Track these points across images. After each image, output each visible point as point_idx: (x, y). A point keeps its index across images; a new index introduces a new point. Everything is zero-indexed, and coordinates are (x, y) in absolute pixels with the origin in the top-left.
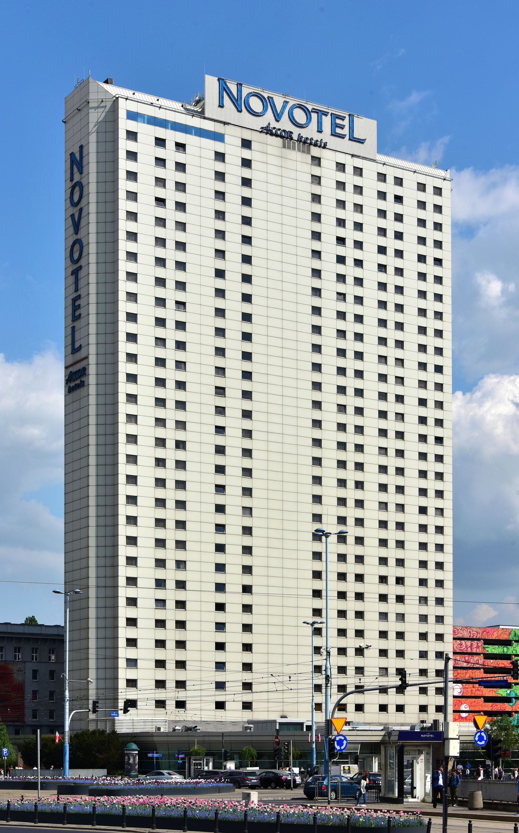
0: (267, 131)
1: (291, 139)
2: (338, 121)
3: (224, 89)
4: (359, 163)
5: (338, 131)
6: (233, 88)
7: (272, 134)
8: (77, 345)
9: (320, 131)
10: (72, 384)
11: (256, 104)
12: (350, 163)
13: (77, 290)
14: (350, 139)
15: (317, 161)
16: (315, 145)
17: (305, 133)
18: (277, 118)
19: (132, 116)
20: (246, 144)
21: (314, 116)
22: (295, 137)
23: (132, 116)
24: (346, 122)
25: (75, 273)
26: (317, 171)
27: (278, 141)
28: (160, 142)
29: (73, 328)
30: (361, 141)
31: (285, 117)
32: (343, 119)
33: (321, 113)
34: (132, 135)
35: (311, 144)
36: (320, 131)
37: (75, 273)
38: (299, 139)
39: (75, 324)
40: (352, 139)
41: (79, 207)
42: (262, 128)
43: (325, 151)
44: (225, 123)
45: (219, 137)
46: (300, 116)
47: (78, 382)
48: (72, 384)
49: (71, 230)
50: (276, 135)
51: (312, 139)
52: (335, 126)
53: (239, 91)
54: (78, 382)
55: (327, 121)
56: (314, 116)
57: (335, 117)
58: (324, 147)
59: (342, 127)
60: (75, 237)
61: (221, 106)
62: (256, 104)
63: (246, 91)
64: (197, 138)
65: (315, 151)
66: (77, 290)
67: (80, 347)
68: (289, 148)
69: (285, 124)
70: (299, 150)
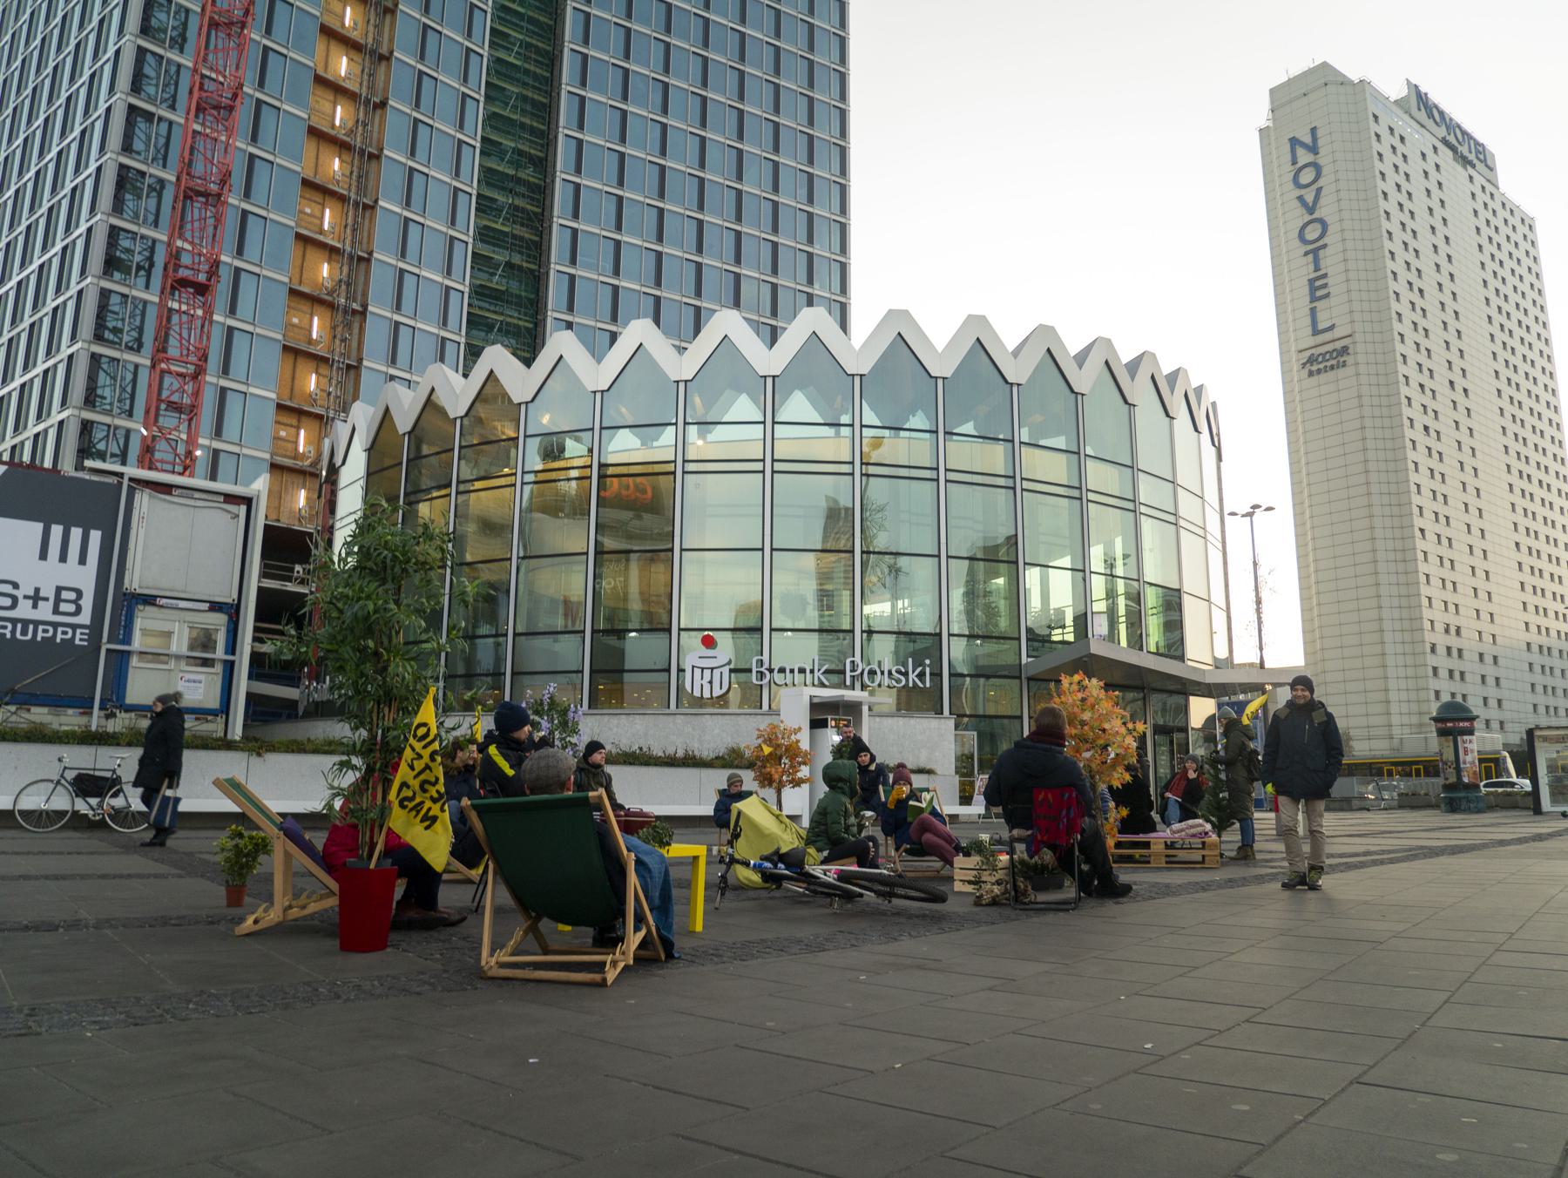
8: (1321, 326)
10: (1314, 368)
13: (1317, 269)
27: (1450, 153)
29: (1313, 311)
39: (1319, 305)
47: (1334, 362)
48: (1314, 368)
49: (1301, 211)
52: (1478, 152)
54: (1334, 362)
60: (1308, 218)
67: (1332, 328)
69: (1451, 139)
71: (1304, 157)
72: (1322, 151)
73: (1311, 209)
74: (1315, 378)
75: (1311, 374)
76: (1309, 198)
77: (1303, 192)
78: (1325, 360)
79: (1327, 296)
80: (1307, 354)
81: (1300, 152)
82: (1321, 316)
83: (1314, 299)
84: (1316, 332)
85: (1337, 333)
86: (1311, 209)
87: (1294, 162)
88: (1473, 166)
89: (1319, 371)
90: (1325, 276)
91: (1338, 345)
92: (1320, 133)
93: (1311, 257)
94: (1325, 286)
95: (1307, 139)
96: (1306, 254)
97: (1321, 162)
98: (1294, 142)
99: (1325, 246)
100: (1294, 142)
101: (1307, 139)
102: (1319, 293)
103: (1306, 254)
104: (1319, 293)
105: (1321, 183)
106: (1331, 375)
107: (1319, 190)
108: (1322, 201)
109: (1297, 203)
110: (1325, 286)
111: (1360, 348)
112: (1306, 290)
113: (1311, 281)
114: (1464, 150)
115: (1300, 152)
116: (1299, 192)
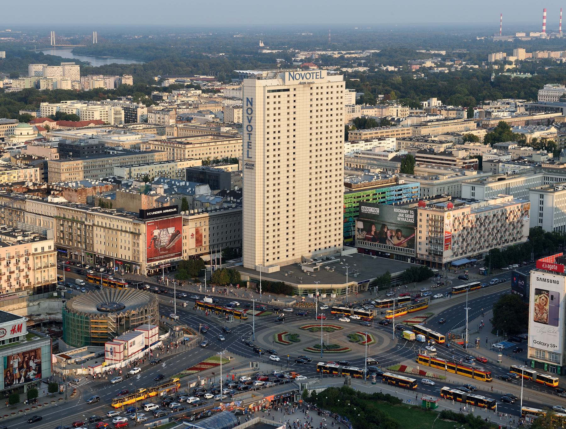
0: (300, 83)
3: (290, 74)
5: (318, 77)
6: (292, 73)
8: (250, 156)
15: (311, 88)
17: (309, 81)
18: (303, 79)
19: (269, 91)
20: (295, 89)
23: (269, 91)
24: (319, 74)
25: (250, 134)
27: (302, 86)
37: (250, 134)
45: (288, 90)
49: (247, 121)
52: (316, 75)
55: (315, 75)
62: (297, 77)
65: (311, 86)
69: (305, 80)
71: (249, 106)
73: (250, 122)
76: (250, 118)
82: (250, 153)
83: (248, 148)
84: (248, 157)
85: (252, 160)
86: (250, 122)
88: (313, 83)
91: (253, 163)
92: (253, 100)
97: (253, 109)
98: (247, 98)
100: (247, 98)
101: (250, 100)
105: (252, 115)
106: (250, 170)
108: (252, 121)
111: (257, 166)
113: (248, 142)
116: (247, 115)
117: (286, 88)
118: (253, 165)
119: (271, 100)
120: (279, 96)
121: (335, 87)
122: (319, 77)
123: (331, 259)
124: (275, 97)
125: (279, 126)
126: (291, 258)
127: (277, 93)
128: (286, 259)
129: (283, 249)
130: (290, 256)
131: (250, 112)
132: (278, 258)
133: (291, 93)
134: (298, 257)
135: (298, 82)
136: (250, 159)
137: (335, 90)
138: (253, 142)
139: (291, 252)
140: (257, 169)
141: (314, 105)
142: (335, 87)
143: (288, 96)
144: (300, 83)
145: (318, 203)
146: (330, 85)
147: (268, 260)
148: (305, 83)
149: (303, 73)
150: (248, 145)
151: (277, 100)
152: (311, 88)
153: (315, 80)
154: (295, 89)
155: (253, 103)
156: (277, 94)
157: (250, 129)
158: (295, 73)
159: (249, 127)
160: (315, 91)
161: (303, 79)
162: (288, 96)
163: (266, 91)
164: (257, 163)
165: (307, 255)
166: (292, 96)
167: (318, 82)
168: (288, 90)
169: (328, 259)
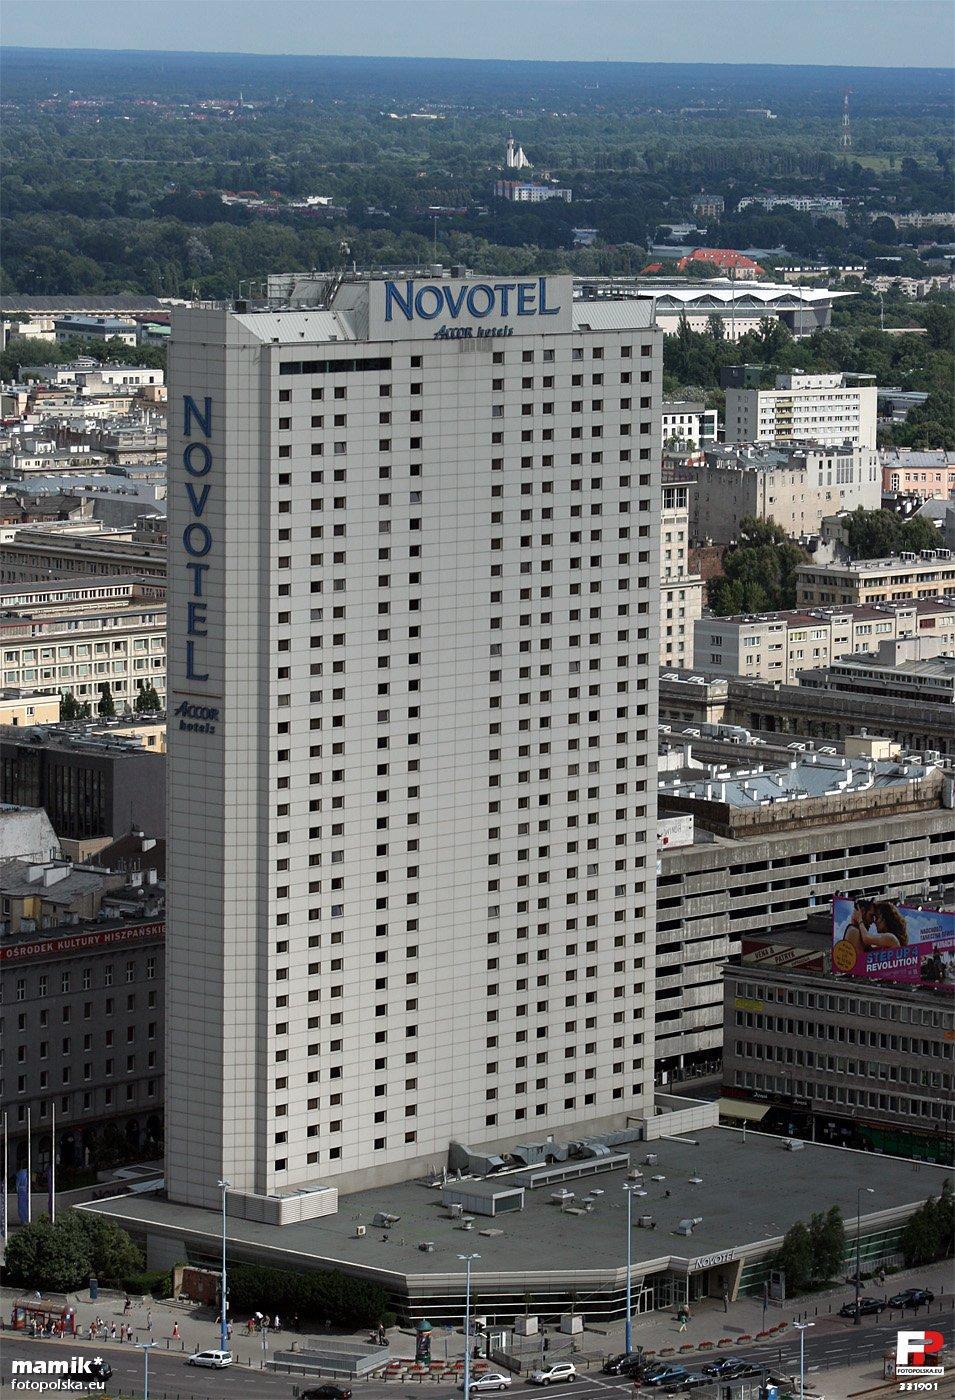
0: (443, 335)
1: (471, 337)
2: (527, 293)
3: (391, 291)
4: (549, 344)
5: (527, 306)
7: (447, 338)
8: (198, 670)
9: (505, 313)
10: (188, 721)
11: (429, 303)
12: (538, 347)
13: (198, 593)
14: (540, 314)
15: (498, 357)
16: (499, 336)
17: (486, 324)
18: (454, 312)
19: (288, 368)
20: (416, 361)
21: (498, 295)
22: (474, 333)
23: (288, 368)
24: (536, 292)
25: (199, 569)
26: (499, 372)
28: (317, 394)
29: (190, 644)
30: (555, 311)
31: (464, 309)
32: (532, 286)
33: (505, 289)
34: (285, 395)
35: (493, 336)
36: (505, 313)
37: (199, 569)
38: (481, 333)
40: (543, 311)
41: (203, 480)
42: (436, 334)
43: (508, 339)
44: (392, 342)
45: (384, 364)
46: (481, 301)
47: (201, 722)
48: (188, 721)
49: (186, 503)
50: (453, 338)
51: (494, 329)
52: (522, 299)
53: (410, 290)
54: (201, 722)
55: (513, 296)
56: (498, 295)
57: (522, 287)
58: (510, 335)
59: (531, 299)
60: (195, 520)
61: (389, 318)
62: (429, 303)
63: (418, 286)
64: (361, 373)
65: (498, 345)
66: (198, 593)
68: (467, 350)
69: (465, 319)
70: (478, 349)
71: (197, 435)
72: (213, 433)
73: (198, 509)
74: (186, 734)
75: (183, 726)
76: (198, 493)
77: (194, 480)
78: (195, 716)
79: (204, 633)
80: (183, 698)
81: (194, 422)
82: (198, 657)
83: (191, 631)
84: (190, 675)
85: (210, 687)
86: (198, 509)
87: (187, 432)
88: (507, 333)
89: (190, 727)
90: (204, 607)
91: (211, 704)
93: (192, 572)
94: (203, 620)
95: (201, 409)
96: (189, 566)
97: (214, 451)
98: (188, 400)
99: (207, 567)
100: (188, 400)
101: (201, 409)
102: (199, 626)
103: (189, 566)
104: (199, 626)
105: (210, 478)
107: (207, 488)
108: (210, 506)
109: (185, 492)
110: (203, 620)
112: (185, 613)
113: (192, 606)
114: (494, 321)
115: (194, 422)
116: (185, 476)
117: (372, 352)
118: (214, 714)
119: (301, 408)
120: (340, 392)
121: (612, 352)
122: (535, 305)
123: (591, 1155)
124: (317, 394)
125: (339, 530)
126: (397, 1151)
127: (329, 376)
128: (371, 1158)
129: (358, 1106)
130: (396, 1140)
131: (198, 461)
132: (335, 1153)
133: (400, 376)
134: (432, 1145)
135: (434, 326)
136: (197, 686)
137: (612, 365)
138: (210, 603)
139: (396, 1126)
140: (229, 729)
141: (512, 437)
142: (612, 352)
143: (385, 390)
144: (443, 335)
145: (534, 892)
146: (588, 343)
147: (281, 1165)
148: (467, 332)
149: (455, 287)
150: (193, 619)
151: (329, 407)
152: (498, 357)
153: (513, 320)
154: (416, 361)
155: (215, 423)
156: (328, 381)
157: (199, 545)
158: (418, 286)
159: (196, 534)
160: (513, 371)
161: (454, 312)
162: (385, 390)
163: (275, 368)
164: (229, 702)
165: (473, 1137)
166: (401, 390)
167: (528, 331)
168: (384, 364)
169: (577, 1154)
